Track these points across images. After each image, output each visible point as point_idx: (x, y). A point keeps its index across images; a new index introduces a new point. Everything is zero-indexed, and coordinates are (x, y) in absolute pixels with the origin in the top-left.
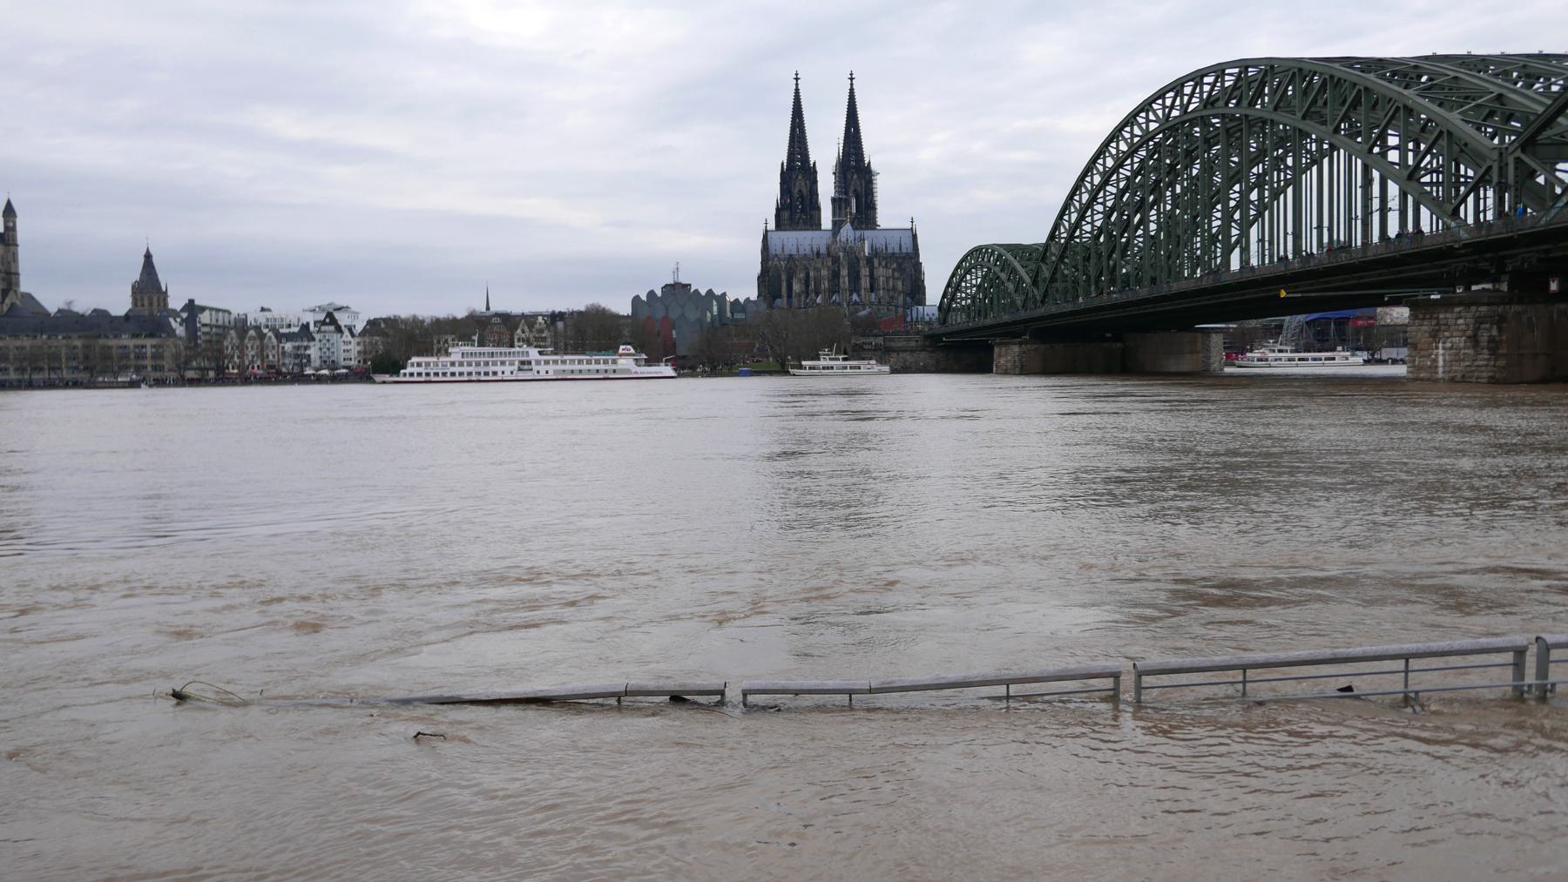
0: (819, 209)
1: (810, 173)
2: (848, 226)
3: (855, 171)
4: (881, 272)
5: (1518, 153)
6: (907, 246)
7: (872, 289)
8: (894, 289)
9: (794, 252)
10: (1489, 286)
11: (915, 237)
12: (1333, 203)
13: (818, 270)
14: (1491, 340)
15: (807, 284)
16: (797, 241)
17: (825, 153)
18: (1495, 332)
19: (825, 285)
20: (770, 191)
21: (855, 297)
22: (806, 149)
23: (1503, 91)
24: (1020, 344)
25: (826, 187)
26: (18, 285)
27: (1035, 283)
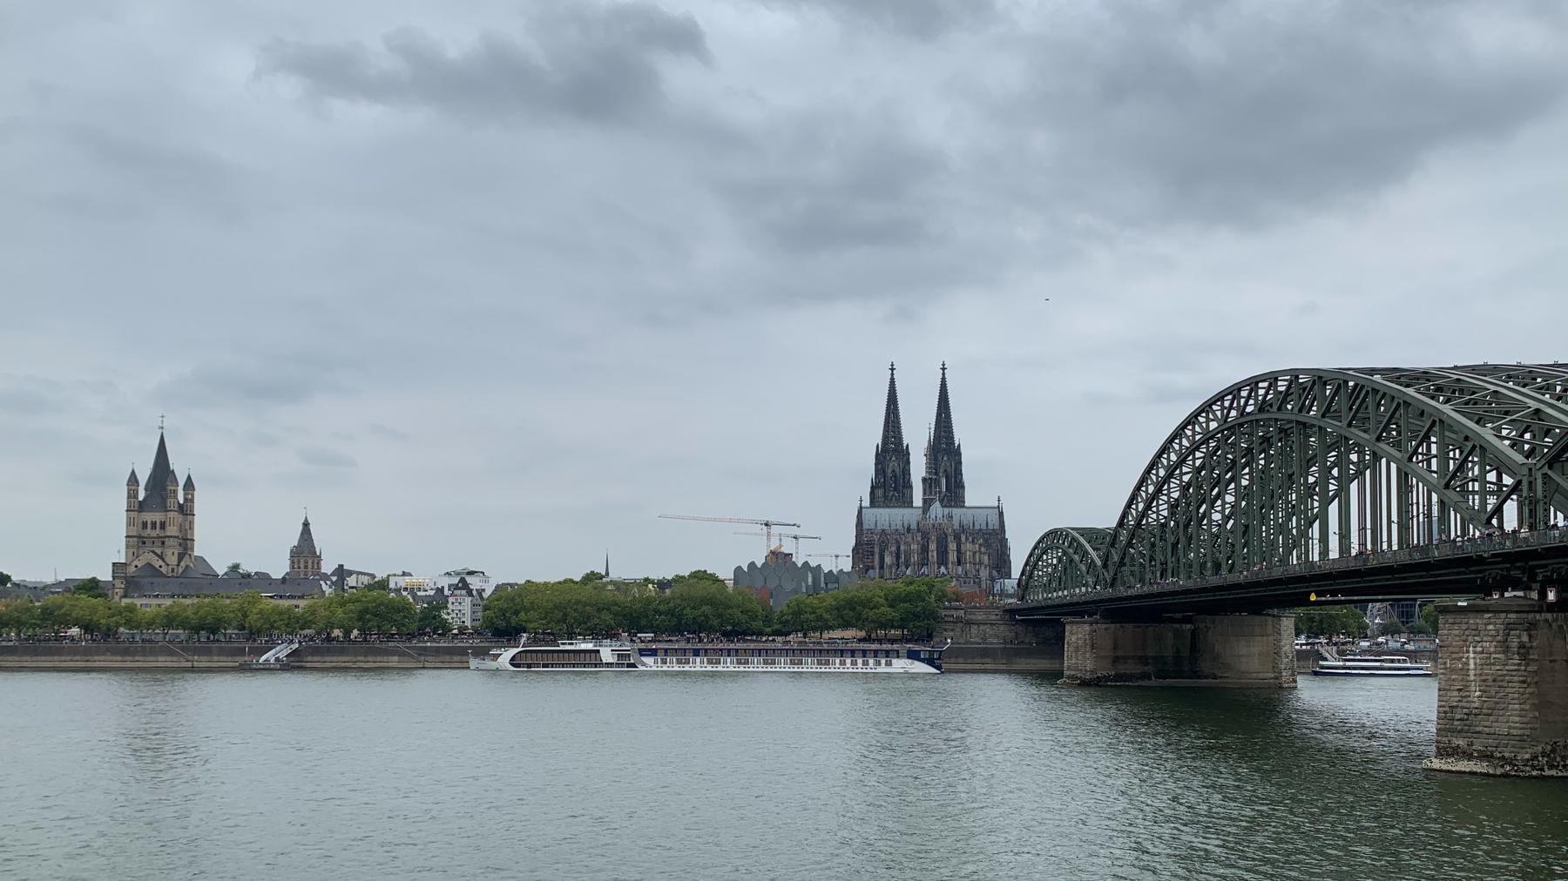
0: (911, 487)
1: (904, 455)
4: (968, 547)
5: (1546, 469)
6: (994, 522)
7: (959, 563)
8: (981, 563)
9: (886, 527)
10: (1520, 594)
11: (1001, 514)
12: (1357, 518)
14: (1522, 646)
15: (898, 557)
17: (917, 435)
18: (1525, 638)
19: (915, 558)
21: (943, 569)
22: (900, 433)
23: (1542, 406)
25: (918, 468)
27: (1105, 566)
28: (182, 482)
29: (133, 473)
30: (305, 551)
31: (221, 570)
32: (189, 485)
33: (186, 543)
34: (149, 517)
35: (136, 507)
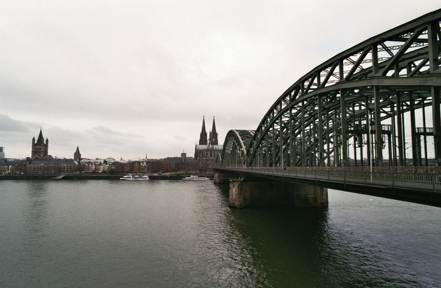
0: (207, 141)
1: (206, 134)
2: (211, 145)
3: (214, 134)
7: (214, 156)
9: (201, 149)
13: (204, 153)
15: (203, 155)
16: (204, 147)
17: (209, 129)
18: (241, 187)
19: (205, 155)
20: (199, 138)
21: (211, 158)
24: (218, 173)
26: (47, 154)
28: (45, 140)
29: (34, 138)
30: (77, 154)
31: (54, 158)
32: (47, 140)
33: (46, 152)
34: (37, 147)
35: (34, 145)
